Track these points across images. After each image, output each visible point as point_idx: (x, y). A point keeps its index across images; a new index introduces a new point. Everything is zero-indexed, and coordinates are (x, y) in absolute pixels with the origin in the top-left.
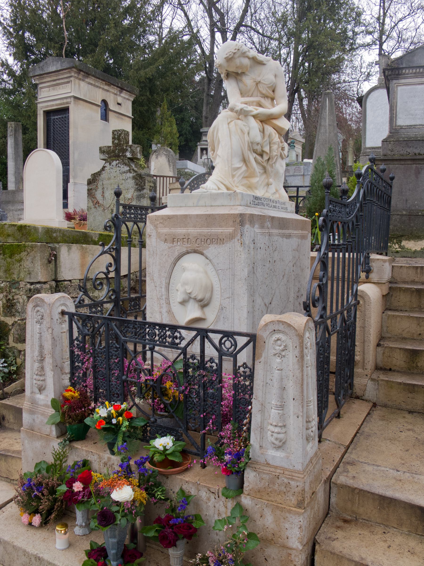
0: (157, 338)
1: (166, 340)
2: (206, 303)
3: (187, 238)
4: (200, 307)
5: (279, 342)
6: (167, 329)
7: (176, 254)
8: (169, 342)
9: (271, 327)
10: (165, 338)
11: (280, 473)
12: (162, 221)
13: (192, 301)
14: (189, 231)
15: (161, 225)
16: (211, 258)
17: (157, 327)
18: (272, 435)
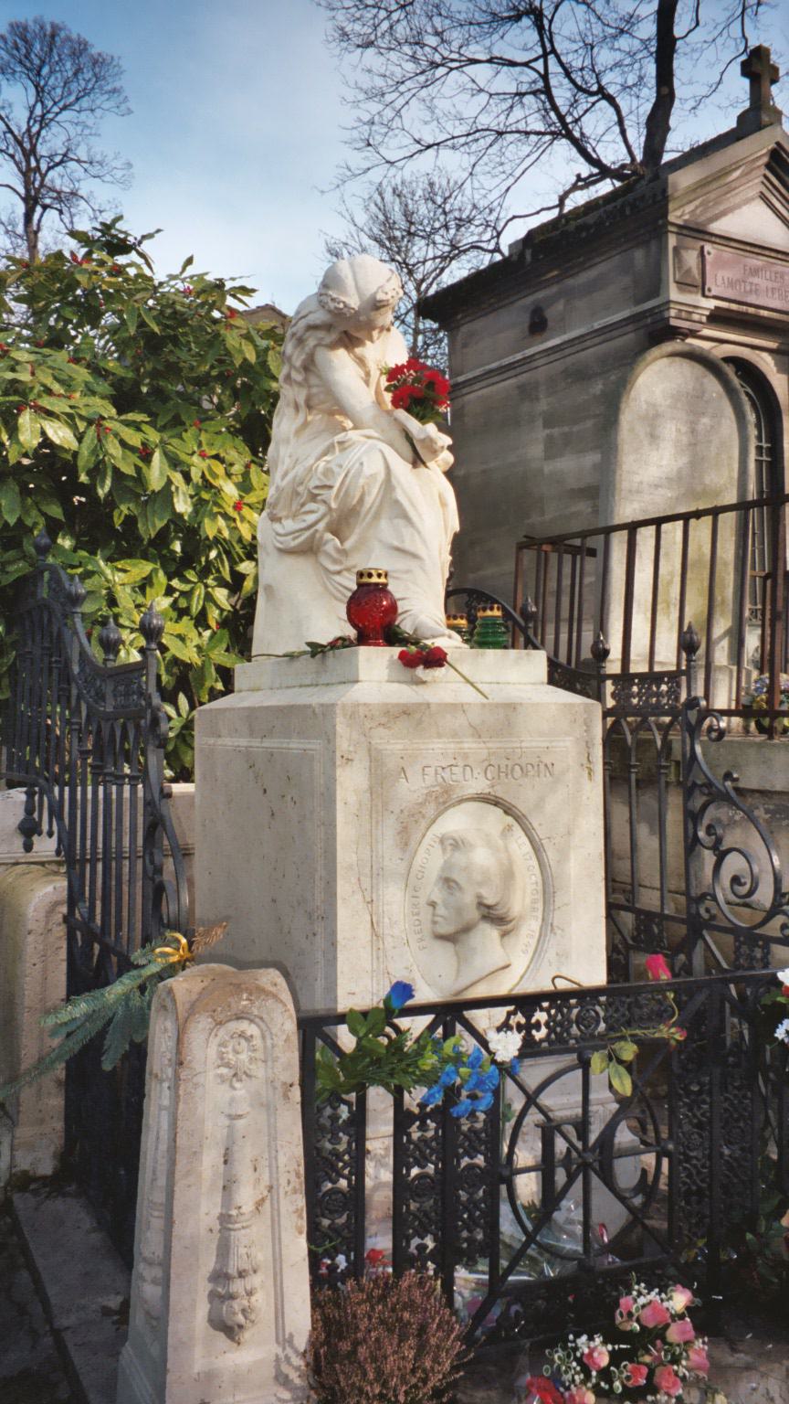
0: (602, 1026)
12: (384, 720)
15: (381, 729)
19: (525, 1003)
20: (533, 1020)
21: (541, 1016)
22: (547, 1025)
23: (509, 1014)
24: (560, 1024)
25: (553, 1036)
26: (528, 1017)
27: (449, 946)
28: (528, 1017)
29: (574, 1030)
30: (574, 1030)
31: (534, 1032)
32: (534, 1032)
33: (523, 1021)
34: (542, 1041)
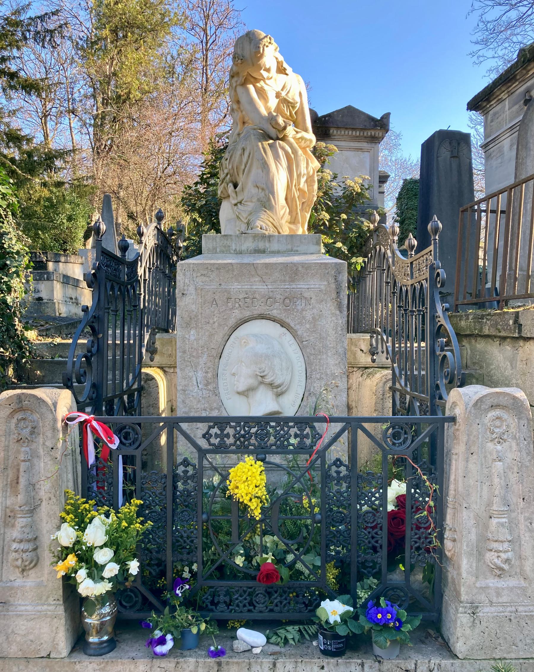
1: (288, 442)
2: (284, 390)
3: (251, 297)
4: (274, 397)
5: (498, 423)
6: (291, 424)
7: (232, 322)
8: (293, 445)
9: (489, 402)
10: (287, 440)
11: (511, 612)
13: (262, 388)
14: (255, 287)
16: (292, 325)
17: (273, 424)
18: (498, 557)
19: (222, 422)
20: (225, 432)
21: (230, 431)
22: (234, 436)
23: (210, 427)
24: (243, 436)
25: (238, 443)
26: (222, 430)
27: (243, 399)
28: (222, 430)
29: (253, 441)
30: (253, 441)
31: (225, 439)
32: (225, 439)
33: (219, 432)
34: (231, 445)
